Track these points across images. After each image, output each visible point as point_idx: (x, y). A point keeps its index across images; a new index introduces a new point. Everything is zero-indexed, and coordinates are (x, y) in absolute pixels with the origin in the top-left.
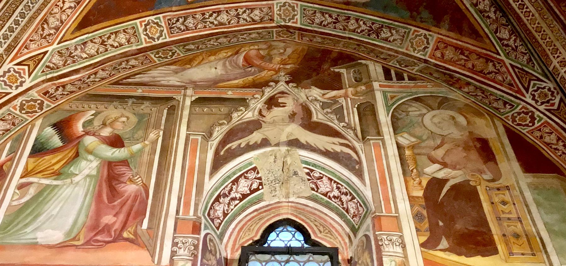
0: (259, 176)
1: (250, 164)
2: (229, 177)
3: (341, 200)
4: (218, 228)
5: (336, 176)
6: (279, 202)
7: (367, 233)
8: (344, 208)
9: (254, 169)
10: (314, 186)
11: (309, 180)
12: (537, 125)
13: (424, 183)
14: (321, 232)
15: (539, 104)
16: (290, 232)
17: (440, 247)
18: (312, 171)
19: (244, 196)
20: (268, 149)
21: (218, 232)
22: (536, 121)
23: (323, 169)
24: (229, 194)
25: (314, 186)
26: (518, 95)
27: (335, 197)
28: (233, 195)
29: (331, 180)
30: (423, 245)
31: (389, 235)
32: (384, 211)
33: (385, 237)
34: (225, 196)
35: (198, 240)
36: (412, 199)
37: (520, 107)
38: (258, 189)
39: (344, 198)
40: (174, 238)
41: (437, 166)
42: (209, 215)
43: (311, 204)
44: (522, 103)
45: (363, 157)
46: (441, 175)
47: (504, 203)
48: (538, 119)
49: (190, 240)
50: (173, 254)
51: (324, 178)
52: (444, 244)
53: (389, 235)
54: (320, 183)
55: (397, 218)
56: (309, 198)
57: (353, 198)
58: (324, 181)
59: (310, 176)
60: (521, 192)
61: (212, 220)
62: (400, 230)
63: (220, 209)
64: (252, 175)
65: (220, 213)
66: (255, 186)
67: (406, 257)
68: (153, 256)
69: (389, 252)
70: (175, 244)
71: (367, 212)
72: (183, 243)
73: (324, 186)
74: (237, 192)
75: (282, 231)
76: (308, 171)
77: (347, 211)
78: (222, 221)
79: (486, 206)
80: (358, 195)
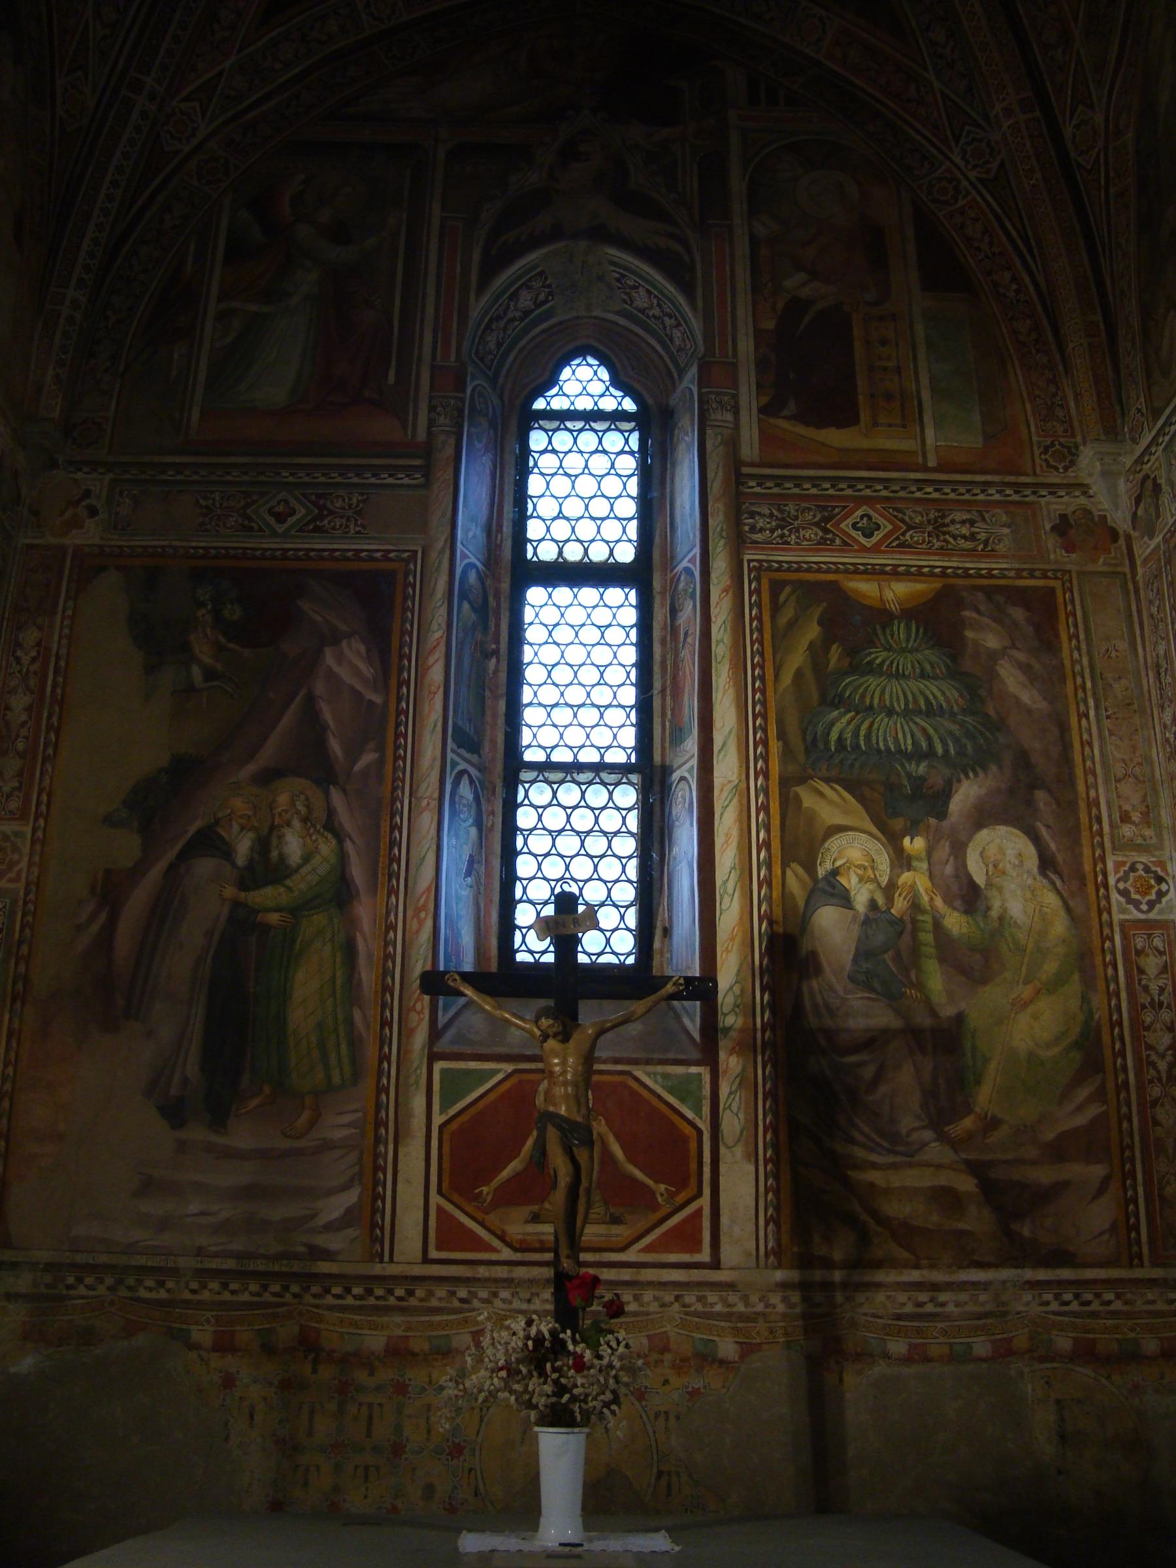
0: (548, 282)
1: (534, 267)
2: (504, 292)
3: (663, 323)
4: (489, 368)
5: (655, 287)
6: (577, 318)
7: (692, 387)
8: (667, 335)
9: (541, 274)
10: (625, 297)
11: (619, 288)
12: (961, 203)
13: (780, 305)
14: (633, 369)
15: (970, 167)
16: (591, 366)
17: (786, 412)
18: (623, 276)
19: (526, 313)
20: (559, 245)
21: (490, 374)
22: (960, 197)
23: (641, 277)
24: (505, 314)
25: (625, 297)
26: (944, 148)
27: (654, 316)
28: (510, 315)
29: (648, 291)
30: (763, 410)
31: (718, 394)
32: (717, 355)
33: (713, 397)
34: (499, 318)
35: (463, 400)
36: (758, 334)
37: (944, 168)
38: (546, 301)
39: (668, 322)
40: (431, 398)
41: (803, 276)
42: (477, 353)
43: (622, 321)
44: (948, 164)
45: (698, 258)
46: (805, 292)
47: (884, 342)
48: (964, 193)
49: (452, 402)
50: (431, 423)
51: (641, 289)
52: (791, 407)
53: (718, 394)
54: (635, 295)
55: (734, 366)
56: (618, 313)
57: (678, 325)
58: (641, 293)
59: (621, 283)
60: (911, 326)
61: (482, 360)
62: (735, 385)
63: (492, 340)
64: (537, 284)
65: (492, 345)
66: (542, 297)
67: (737, 427)
68: (405, 428)
69: (715, 420)
70: (432, 409)
71: (694, 351)
72: (443, 406)
73: (641, 300)
74: (516, 309)
75: (579, 365)
76: (618, 276)
77: (671, 339)
78: (495, 356)
79: (858, 348)
80: (686, 322)
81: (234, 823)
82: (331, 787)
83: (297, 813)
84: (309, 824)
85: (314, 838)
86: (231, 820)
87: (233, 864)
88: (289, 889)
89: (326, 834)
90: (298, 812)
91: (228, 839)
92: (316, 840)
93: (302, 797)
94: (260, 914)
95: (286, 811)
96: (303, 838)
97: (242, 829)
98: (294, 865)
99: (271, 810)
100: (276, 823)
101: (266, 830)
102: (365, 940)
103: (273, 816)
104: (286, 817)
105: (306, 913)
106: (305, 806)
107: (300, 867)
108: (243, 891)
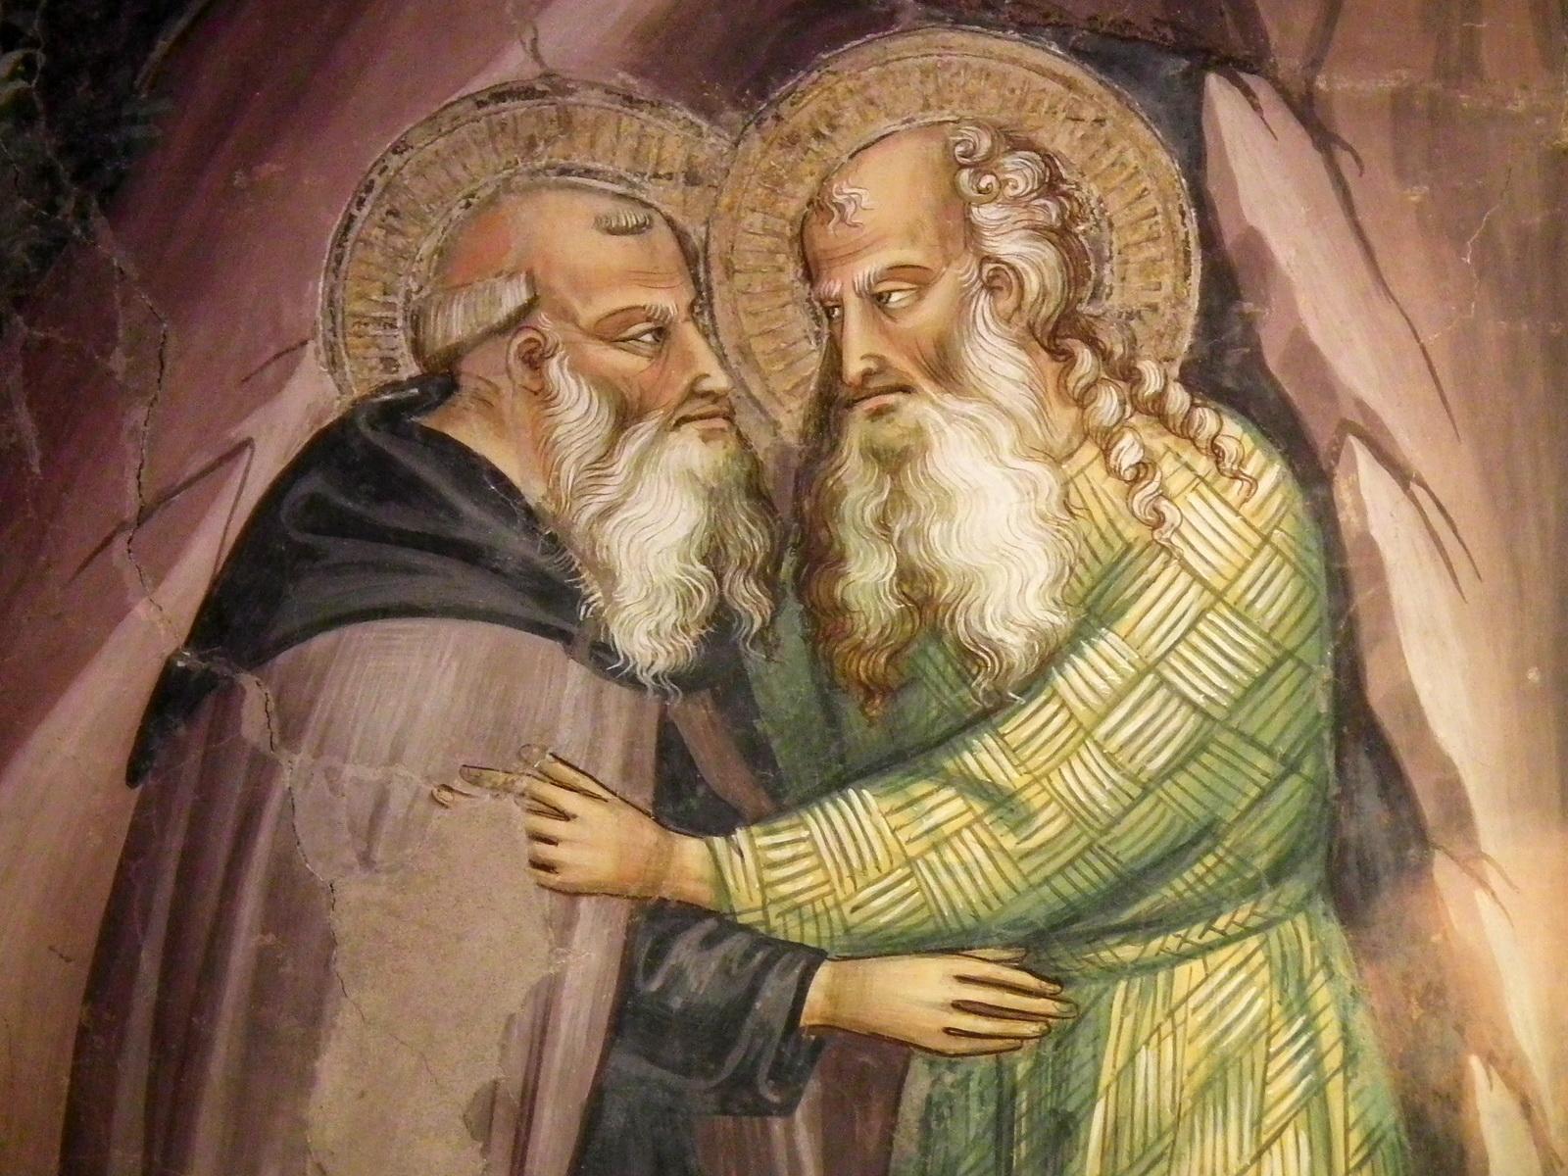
81: (553, 368)
82: (1214, 83)
83: (990, 288)
84: (1086, 360)
85: (1128, 453)
86: (534, 359)
87: (602, 656)
88: (998, 800)
89: (1208, 420)
90: (998, 278)
91: (534, 491)
92: (1145, 468)
93: (1019, 173)
94: (823, 974)
95: (920, 280)
96: (1056, 460)
97: (626, 415)
98: (1016, 645)
99: (811, 273)
100: (854, 366)
101: (791, 418)
102: (1526, 1107)
103: (829, 312)
104: (927, 314)
105: (1128, 952)
106: (1040, 232)
107: (1051, 658)
108: (699, 827)
